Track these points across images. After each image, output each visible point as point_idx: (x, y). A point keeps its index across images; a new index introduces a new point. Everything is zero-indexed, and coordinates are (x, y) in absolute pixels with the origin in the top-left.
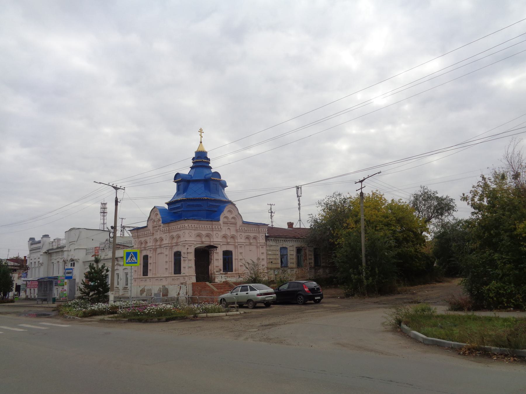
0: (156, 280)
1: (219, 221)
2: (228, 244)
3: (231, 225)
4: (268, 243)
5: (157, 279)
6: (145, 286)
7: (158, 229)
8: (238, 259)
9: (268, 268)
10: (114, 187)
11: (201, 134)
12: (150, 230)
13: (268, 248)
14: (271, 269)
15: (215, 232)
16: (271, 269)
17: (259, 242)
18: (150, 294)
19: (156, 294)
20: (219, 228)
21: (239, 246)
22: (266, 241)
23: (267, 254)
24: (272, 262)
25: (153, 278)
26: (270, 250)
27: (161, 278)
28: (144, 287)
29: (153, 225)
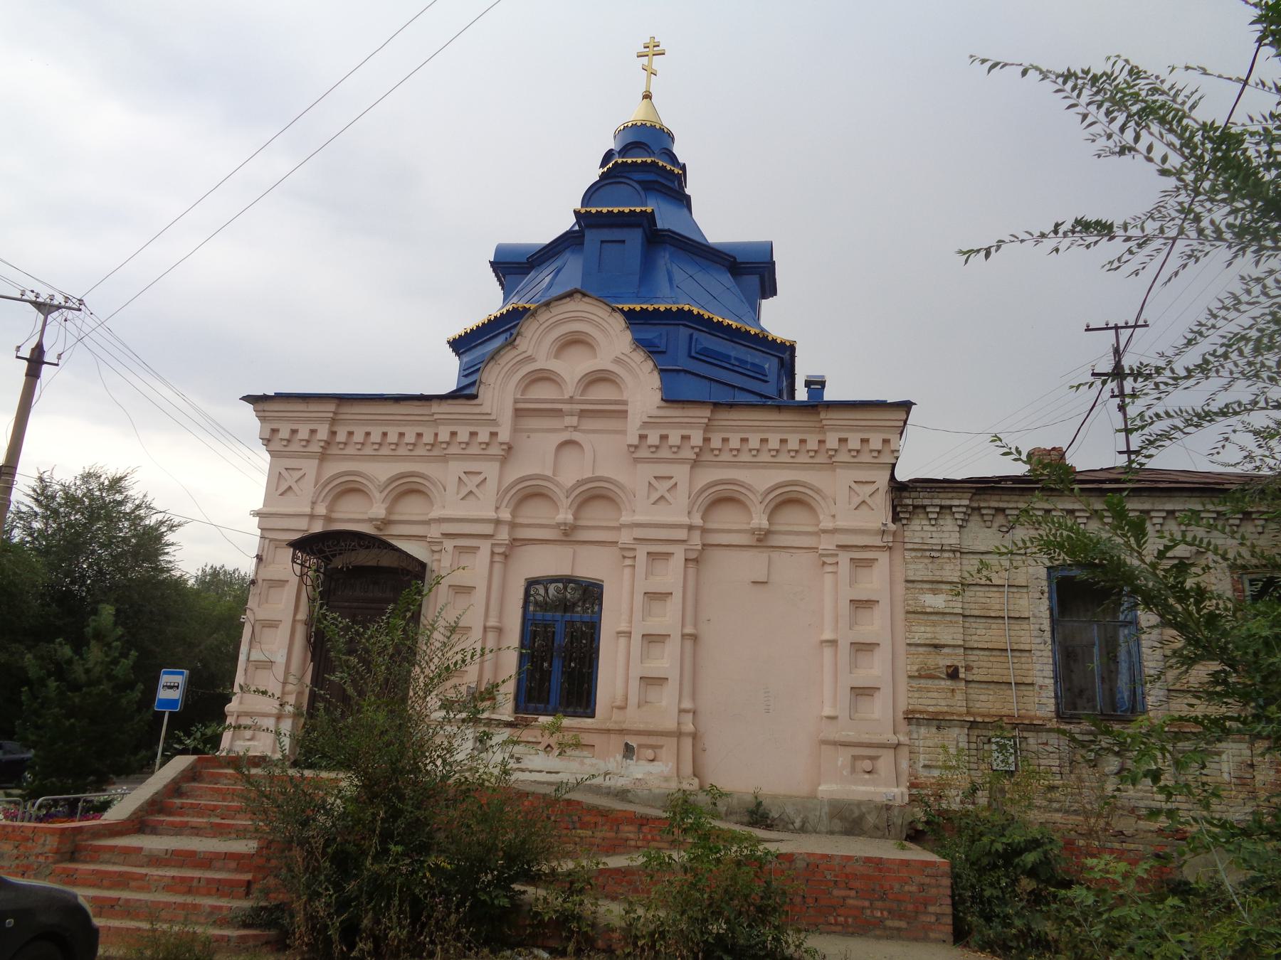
1: (475, 397)
2: (568, 535)
3: (588, 424)
4: (919, 530)
8: (628, 634)
9: (912, 718)
10: (36, 304)
11: (650, 62)
13: (920, 570)
14: (938, 721)
15: (456, 469)
16: (938, 721)
17: (827, 524)
20: (484, 436)
21: (642, 552)
22: (896, 518)
23: (916, 613)
24: (953, 674)
26: (935, 585)
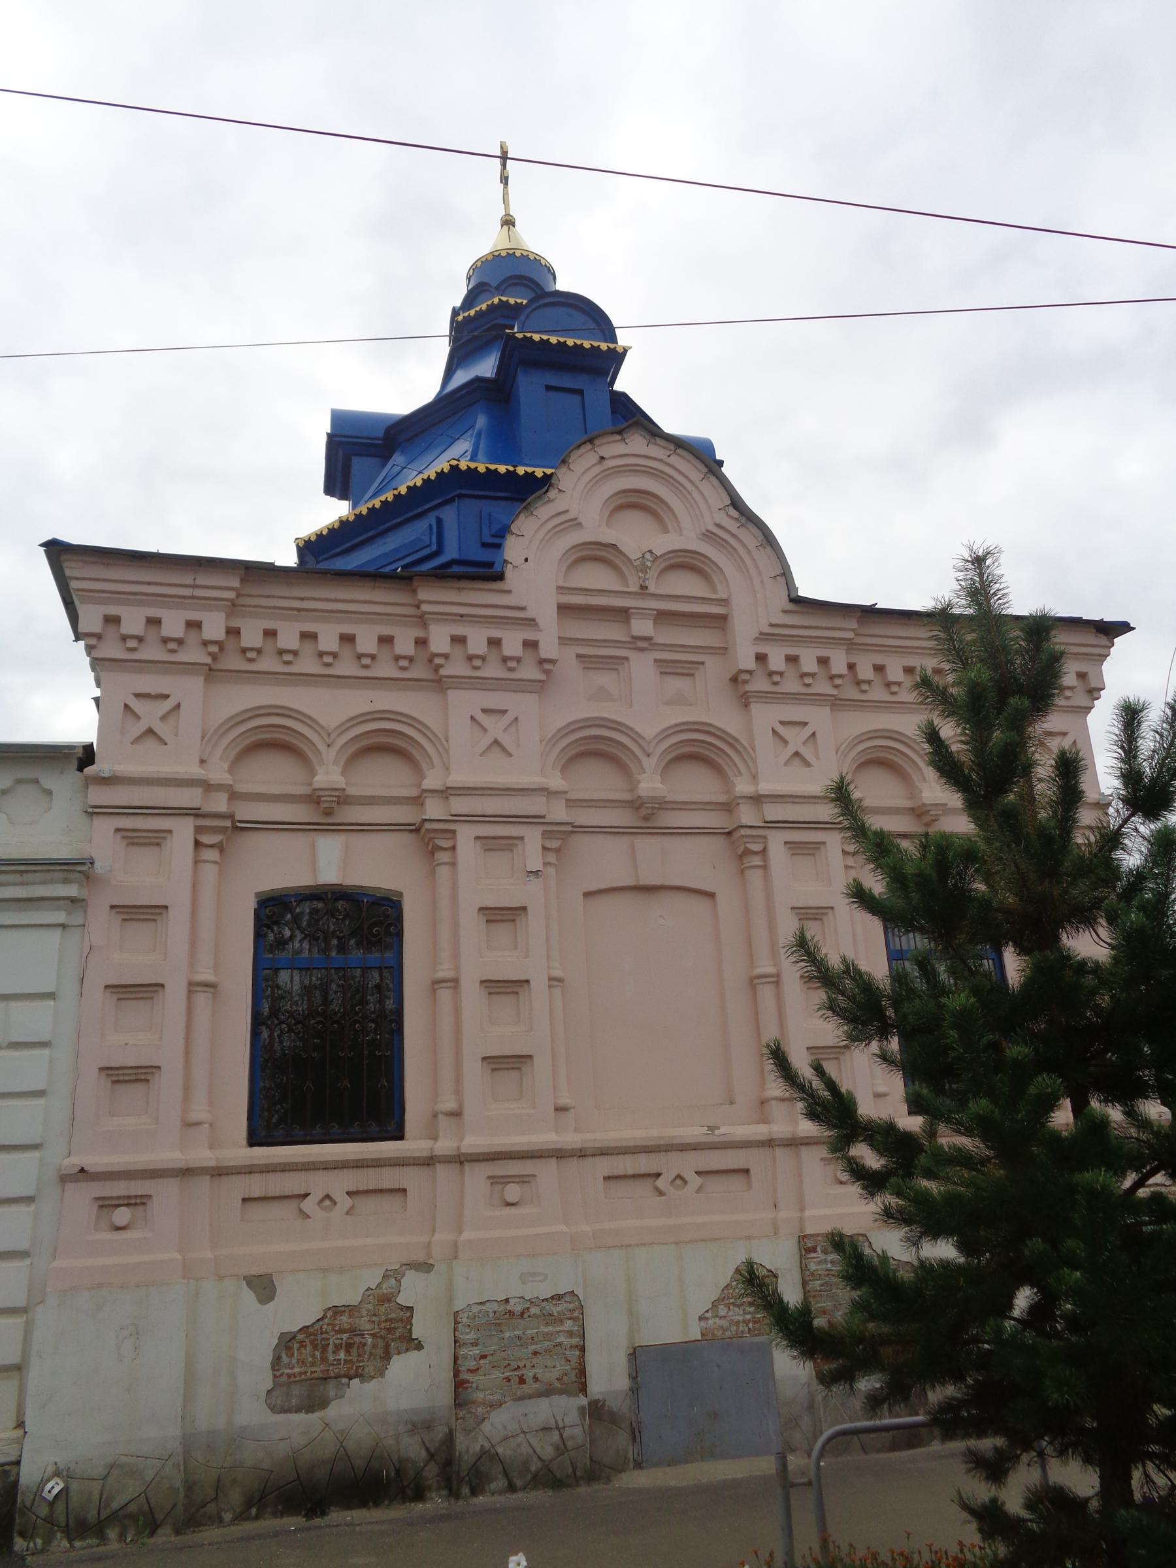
0: (607, 1179)
5: (626, 1164)
6: (391, 1275)
7: (641, 643)
12: (531, 623)
18: (554, 1370)
19: (665, 1352)
25: (560, 1154)
27: (715, 1160)
28: (372, 1278)
29: (561, 583)
